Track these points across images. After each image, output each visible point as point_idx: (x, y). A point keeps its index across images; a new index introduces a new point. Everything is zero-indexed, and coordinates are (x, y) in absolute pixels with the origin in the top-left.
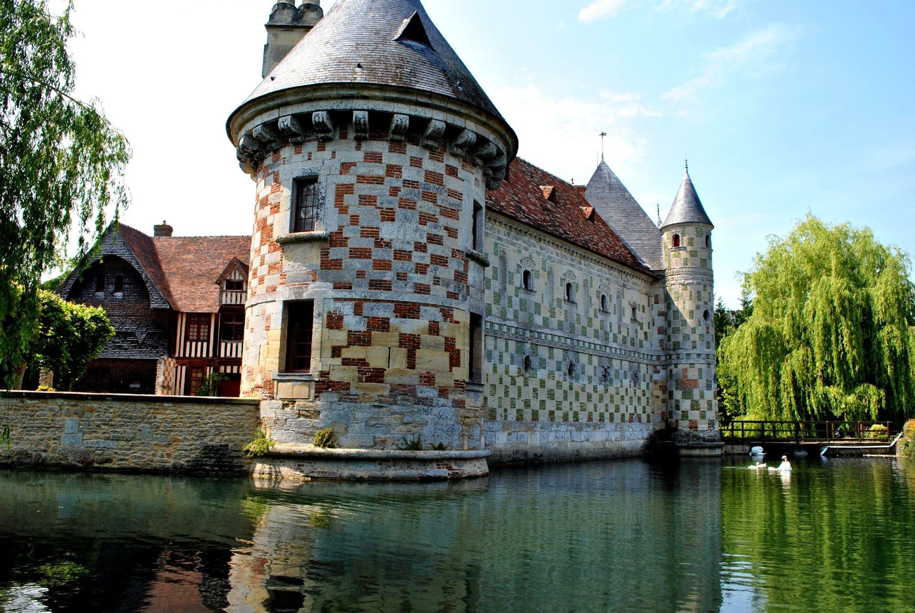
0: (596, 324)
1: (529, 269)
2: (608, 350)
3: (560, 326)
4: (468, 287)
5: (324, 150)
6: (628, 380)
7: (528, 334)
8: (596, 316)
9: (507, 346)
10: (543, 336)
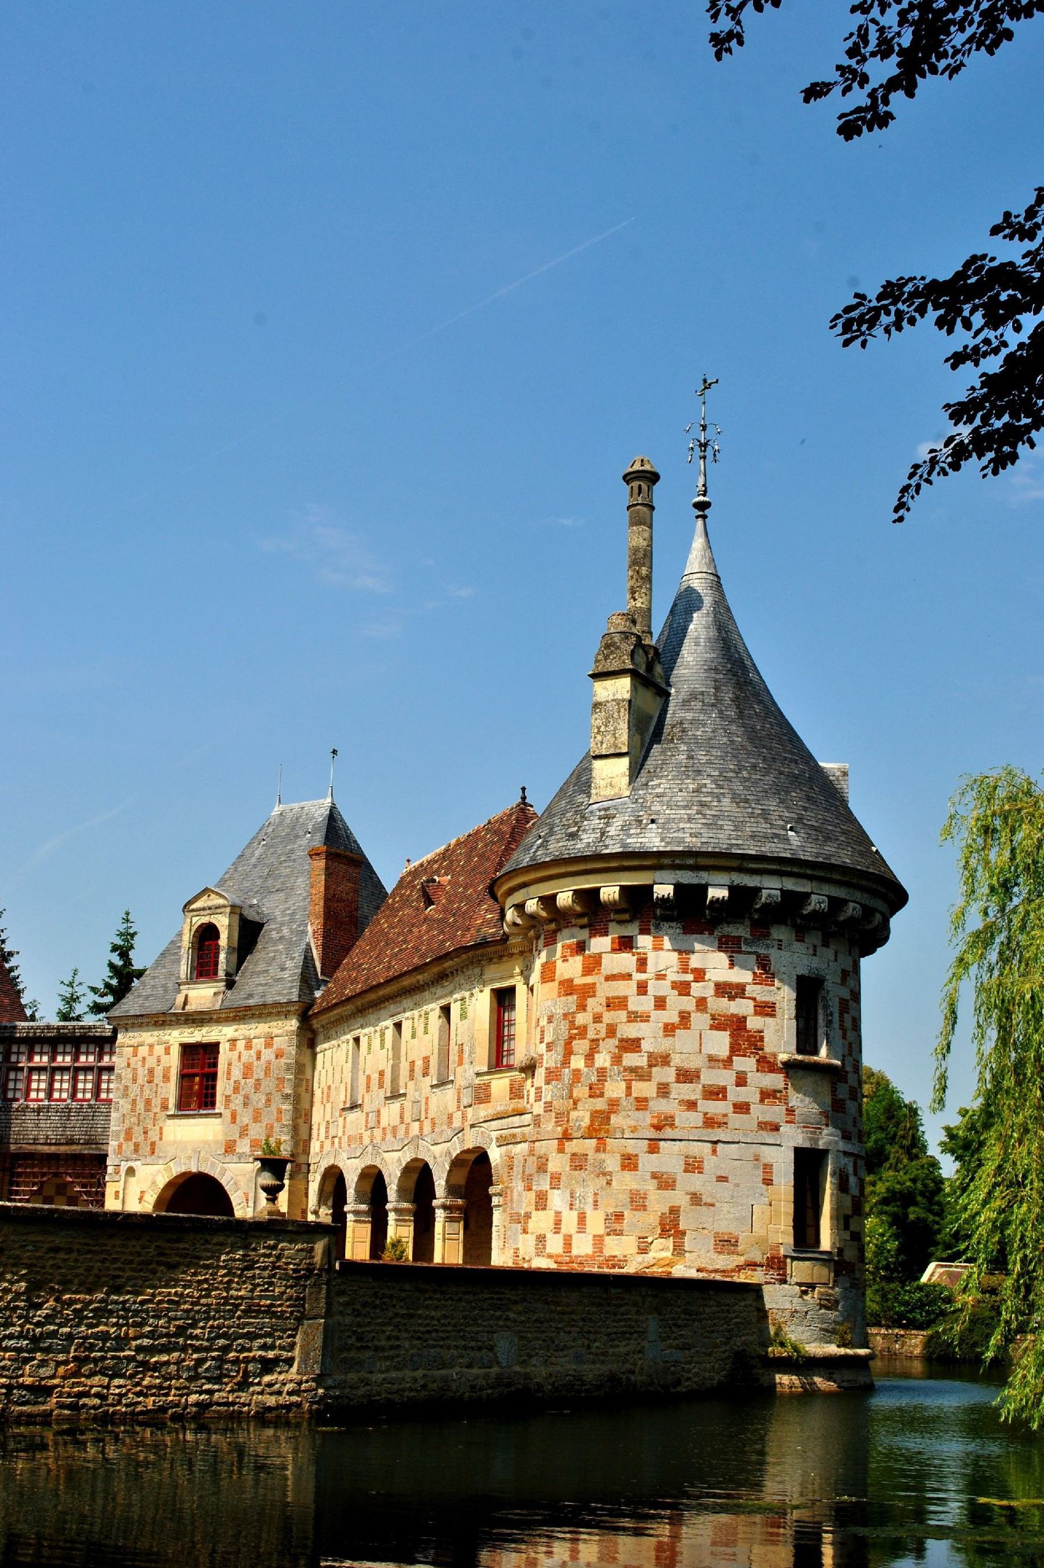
5: (828, 947)
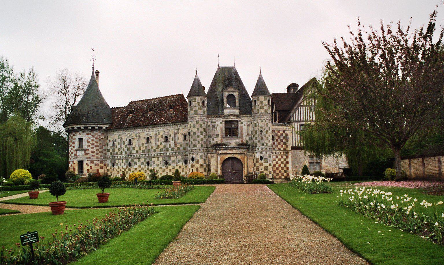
0: (161, 147)
1: (130, 139)
2: (168, 154)
3: (143, 151)
4: (77, 156)
6: (181, 163)
7: (130, 157)
8: (161, 144)
9: (123, 161)
10: (135, 156)
